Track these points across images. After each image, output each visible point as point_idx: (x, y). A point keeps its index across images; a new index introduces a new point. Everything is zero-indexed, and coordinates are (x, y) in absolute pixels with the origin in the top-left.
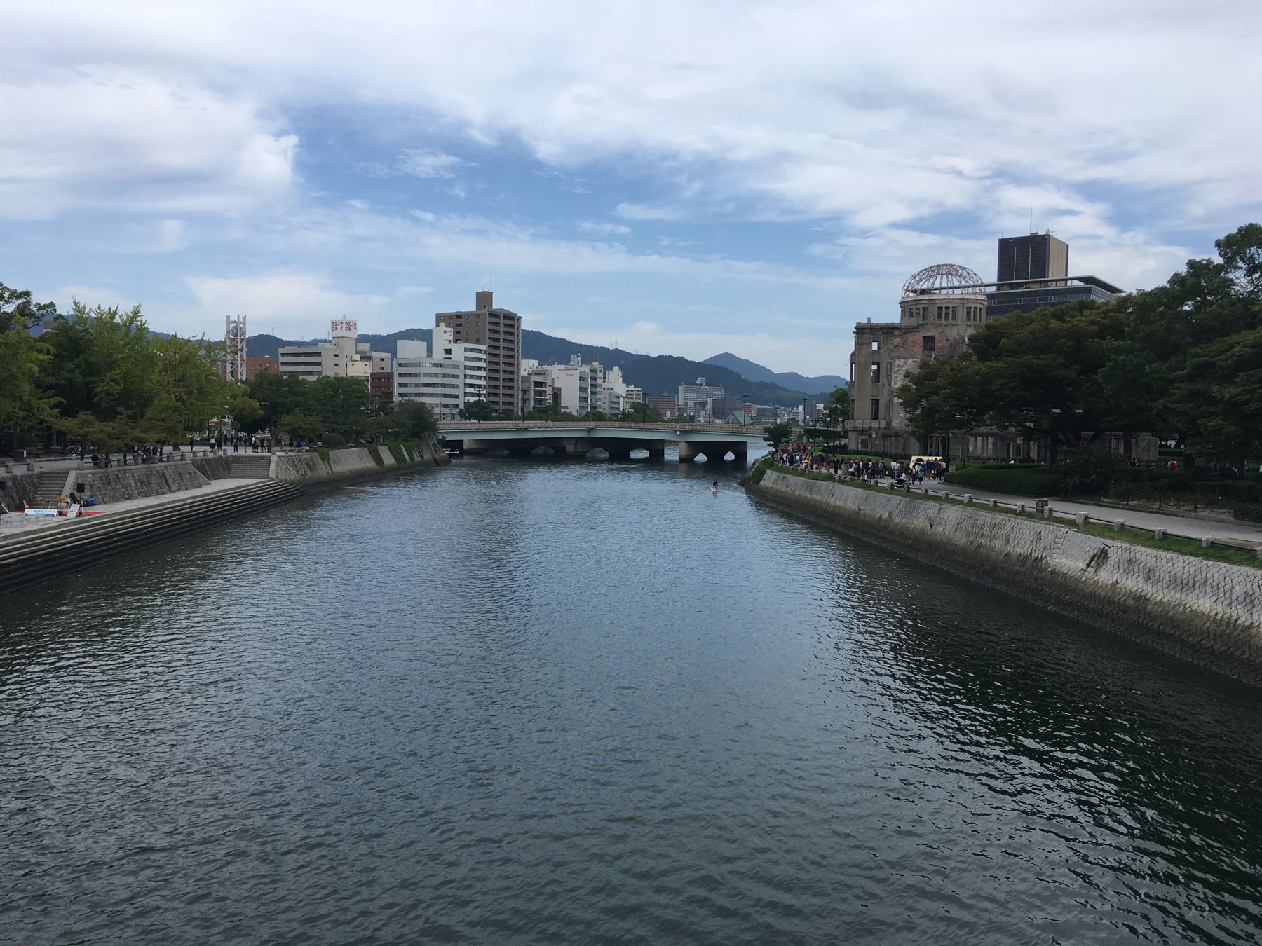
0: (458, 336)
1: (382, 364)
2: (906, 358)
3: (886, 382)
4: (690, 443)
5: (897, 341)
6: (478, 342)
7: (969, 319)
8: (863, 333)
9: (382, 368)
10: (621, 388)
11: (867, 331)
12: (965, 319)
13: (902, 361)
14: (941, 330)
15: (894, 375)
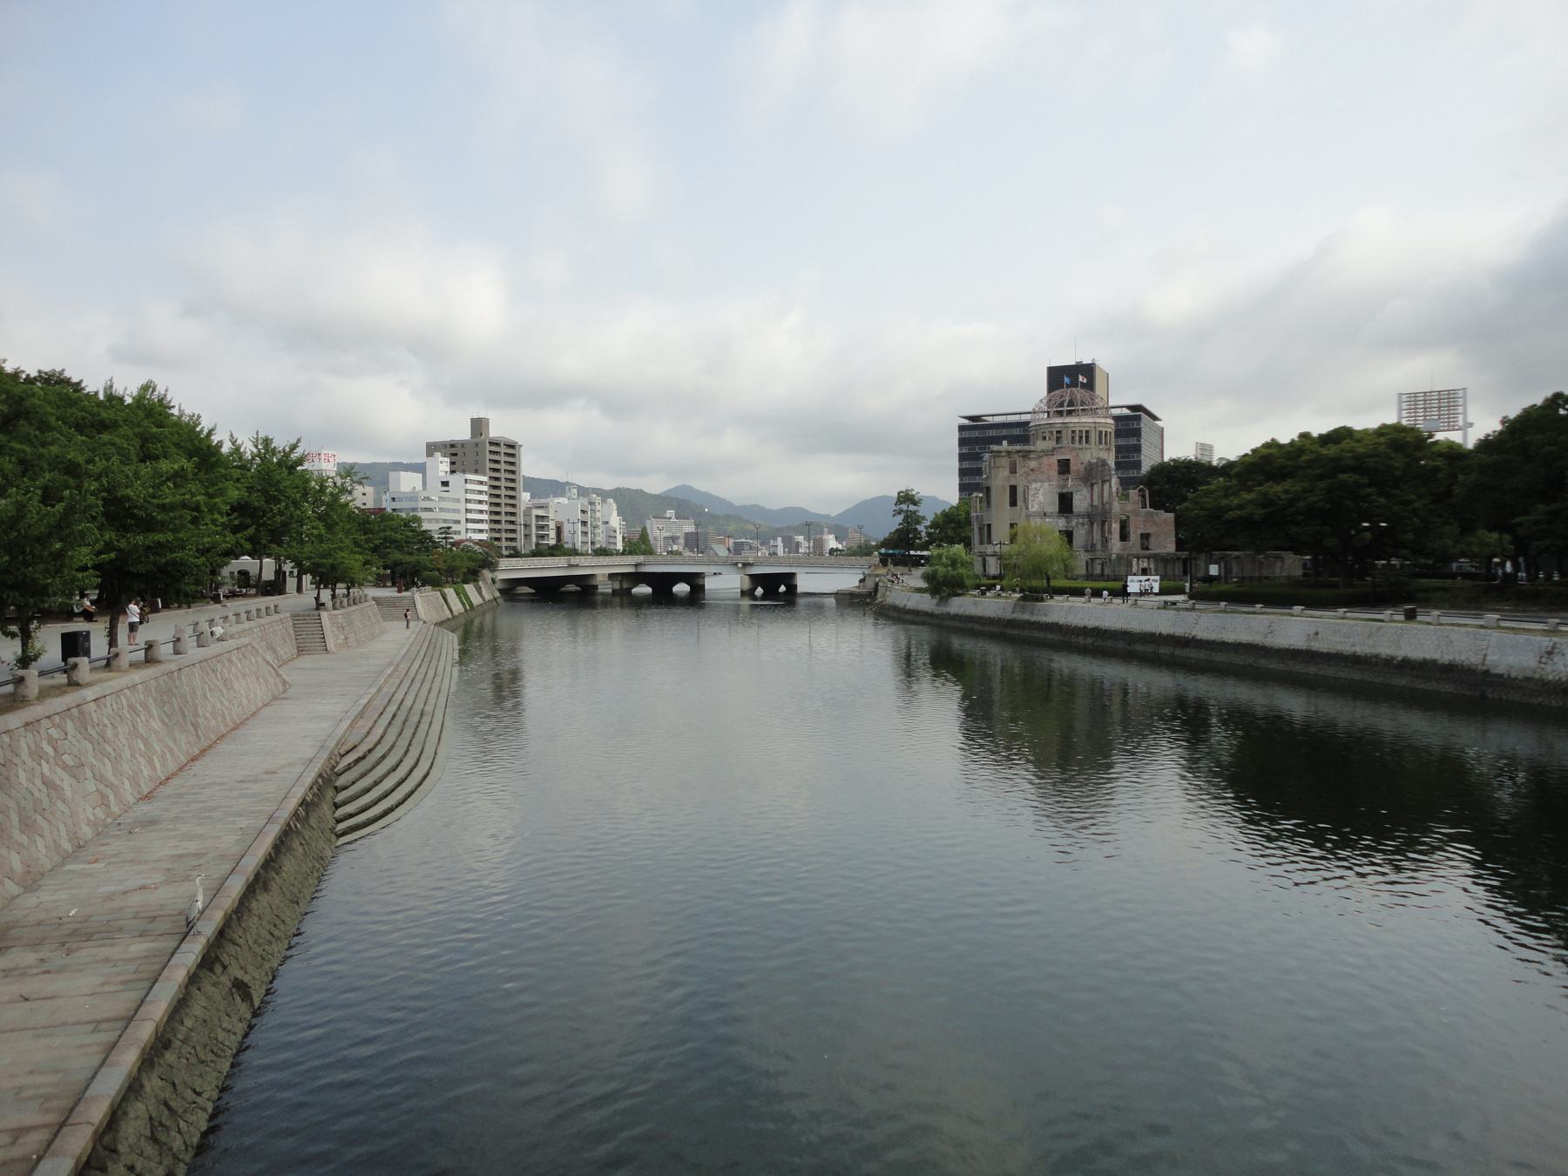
0: (454, 467)
1: (364, 499)
2: (1042, 481)
3: (1023, 505)
4: (750, 576)
5: (1033, 464)
6: (476, 472)
7: (1100, 442)
8: (999, 456)
9: (364, 504)
10: (615, 521)
11: (1003, 454)
12: (1097, 443)
13: (1039, 484)
14: (1075, 454)
15: (1031, 499)
